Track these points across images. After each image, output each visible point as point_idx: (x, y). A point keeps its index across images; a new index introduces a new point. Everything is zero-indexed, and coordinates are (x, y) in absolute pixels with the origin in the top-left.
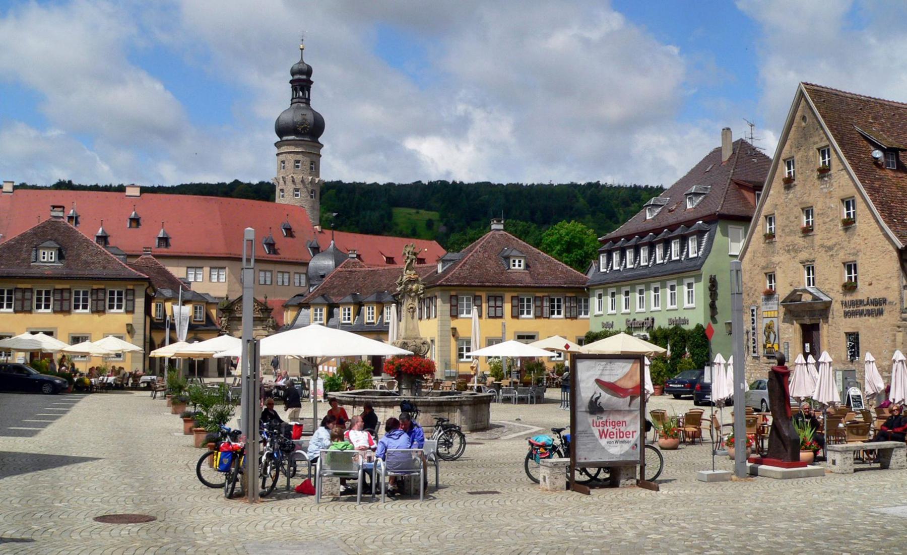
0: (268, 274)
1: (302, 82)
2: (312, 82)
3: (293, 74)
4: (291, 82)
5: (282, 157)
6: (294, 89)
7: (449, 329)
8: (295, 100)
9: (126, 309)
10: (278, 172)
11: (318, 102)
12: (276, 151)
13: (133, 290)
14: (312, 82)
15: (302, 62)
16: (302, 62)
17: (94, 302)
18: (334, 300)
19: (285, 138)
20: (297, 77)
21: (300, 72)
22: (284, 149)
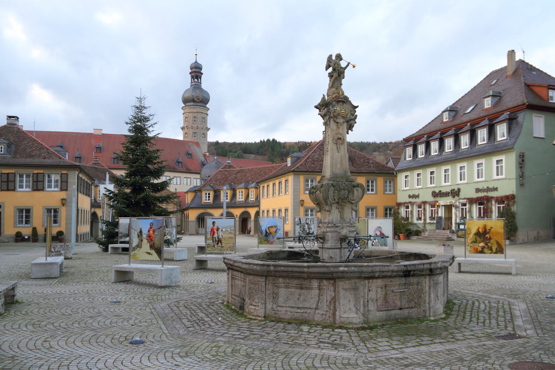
0: (179, 179)
1: (196, 72)
2: (202, 74)
3: (191, 69)
4: (190, 73)
5: (186, 115)
6: (192, 77)
7: (299, 201)
8: (193, 84)
9: (61, 188)
10: (184, 124)
11: (205, 84)
12: (183, 112)
13: (67, 174)
14: (202, 74)
15: (196, 62)
16: (196, 62)
17: (35, 183)
18: (217, 187)
19: (188, 104)
20: (194, 70)
21: (196, 68)
22: (187, 110)
